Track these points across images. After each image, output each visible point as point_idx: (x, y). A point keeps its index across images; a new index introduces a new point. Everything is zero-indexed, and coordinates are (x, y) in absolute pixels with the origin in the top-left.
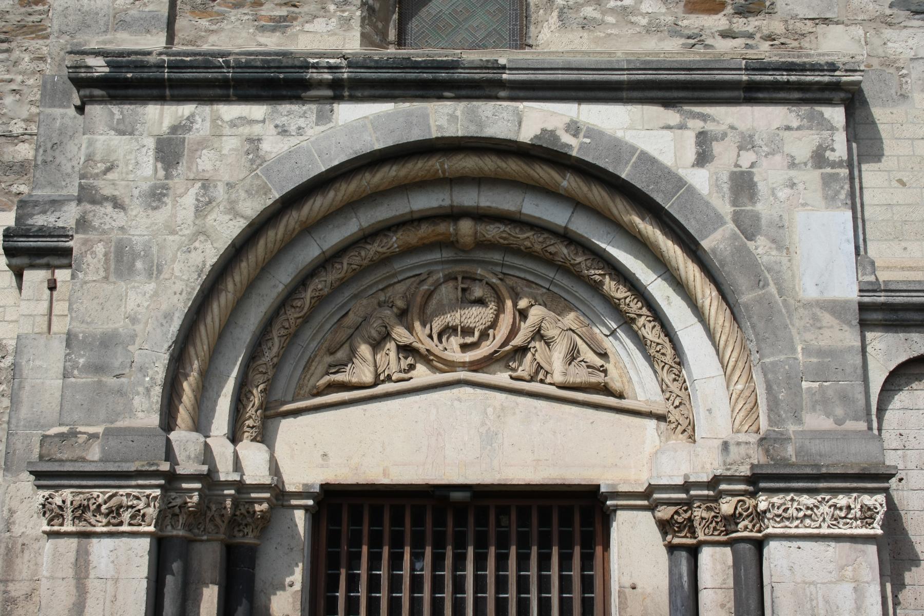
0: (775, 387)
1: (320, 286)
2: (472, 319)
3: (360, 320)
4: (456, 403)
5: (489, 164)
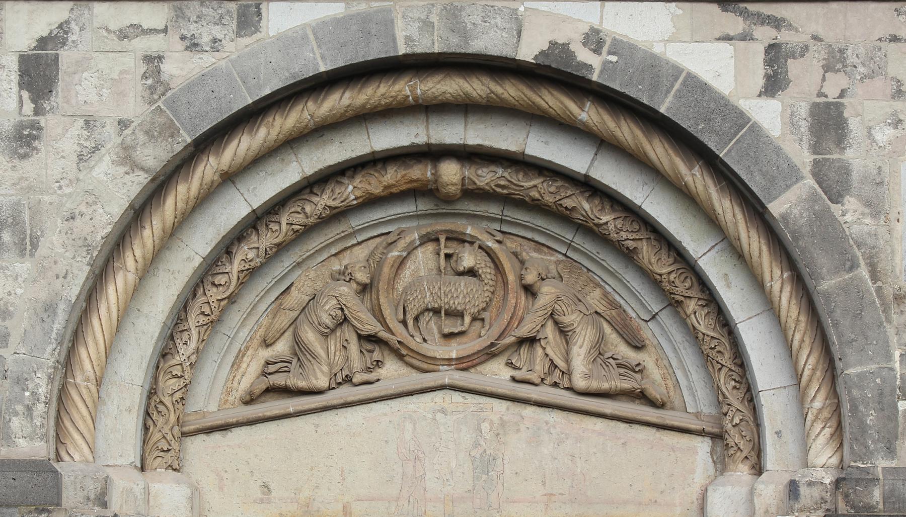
0: (861, 408)
1: (251, 255)
2: (460, 300)
3: (307, 298)
4: (439, 416)
5: (477, 87)
